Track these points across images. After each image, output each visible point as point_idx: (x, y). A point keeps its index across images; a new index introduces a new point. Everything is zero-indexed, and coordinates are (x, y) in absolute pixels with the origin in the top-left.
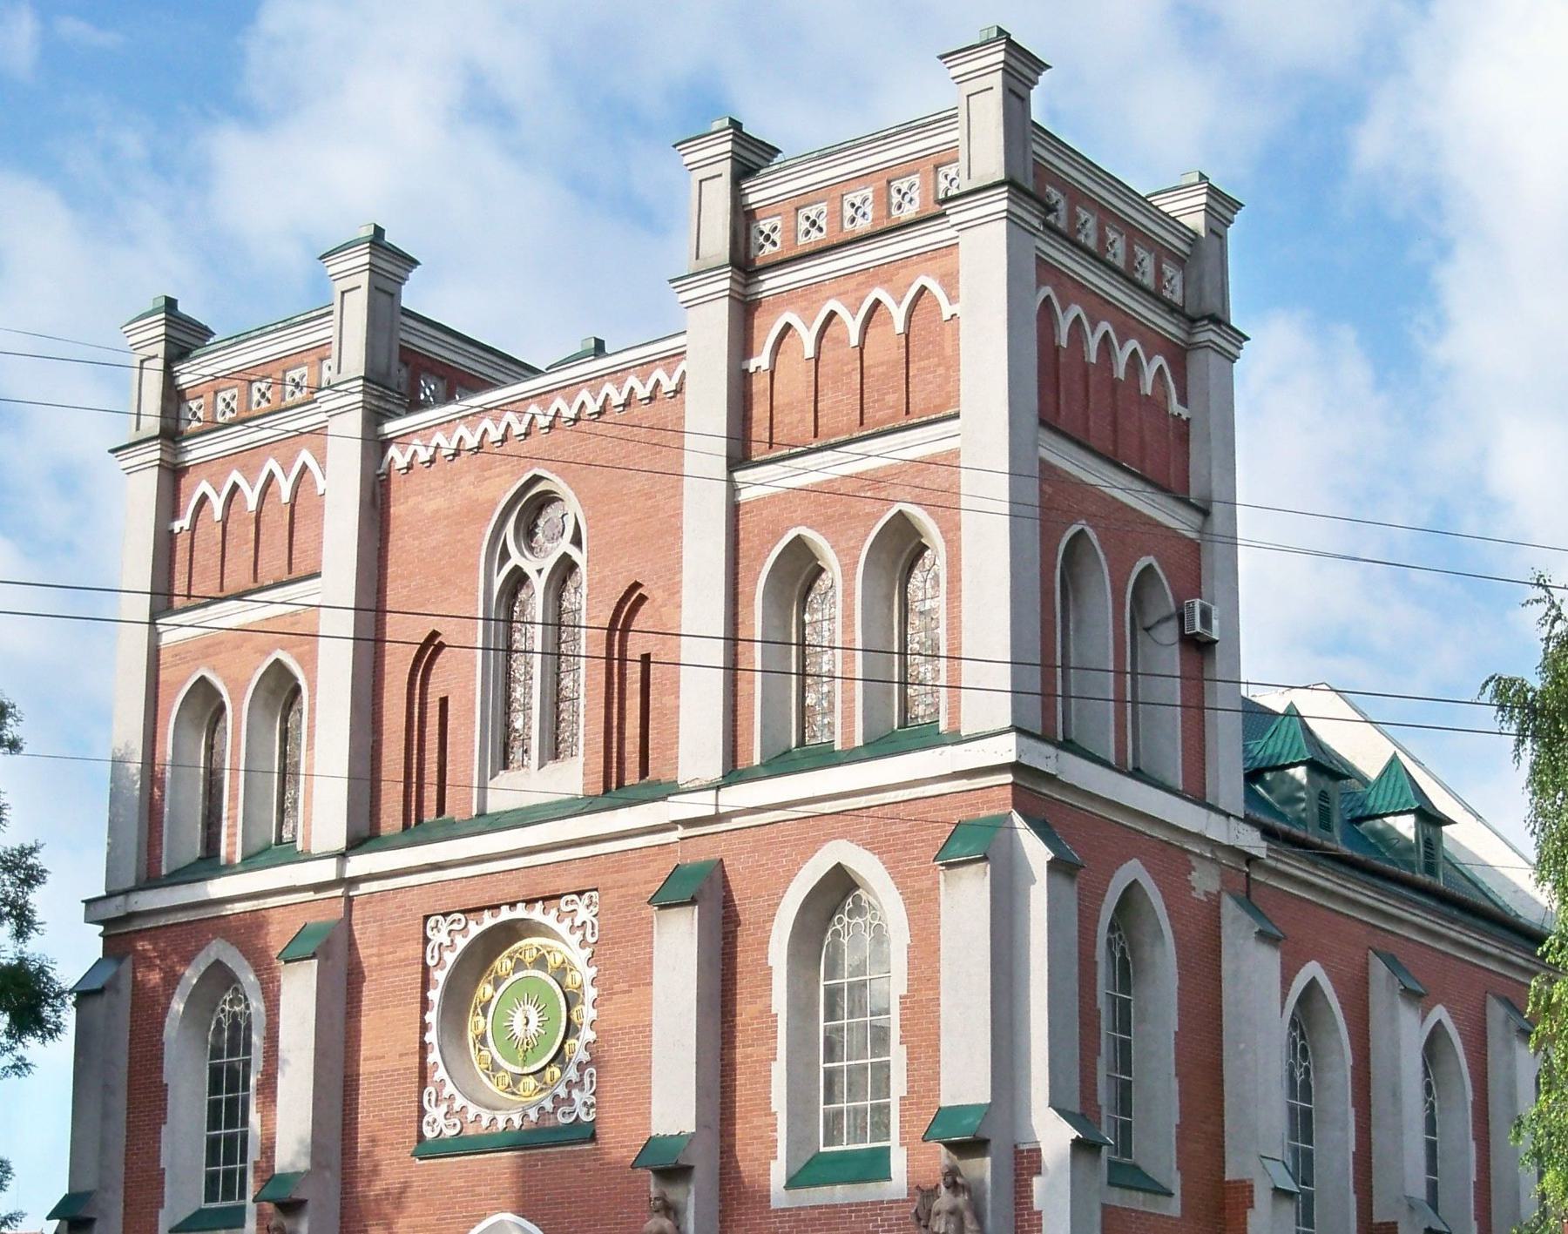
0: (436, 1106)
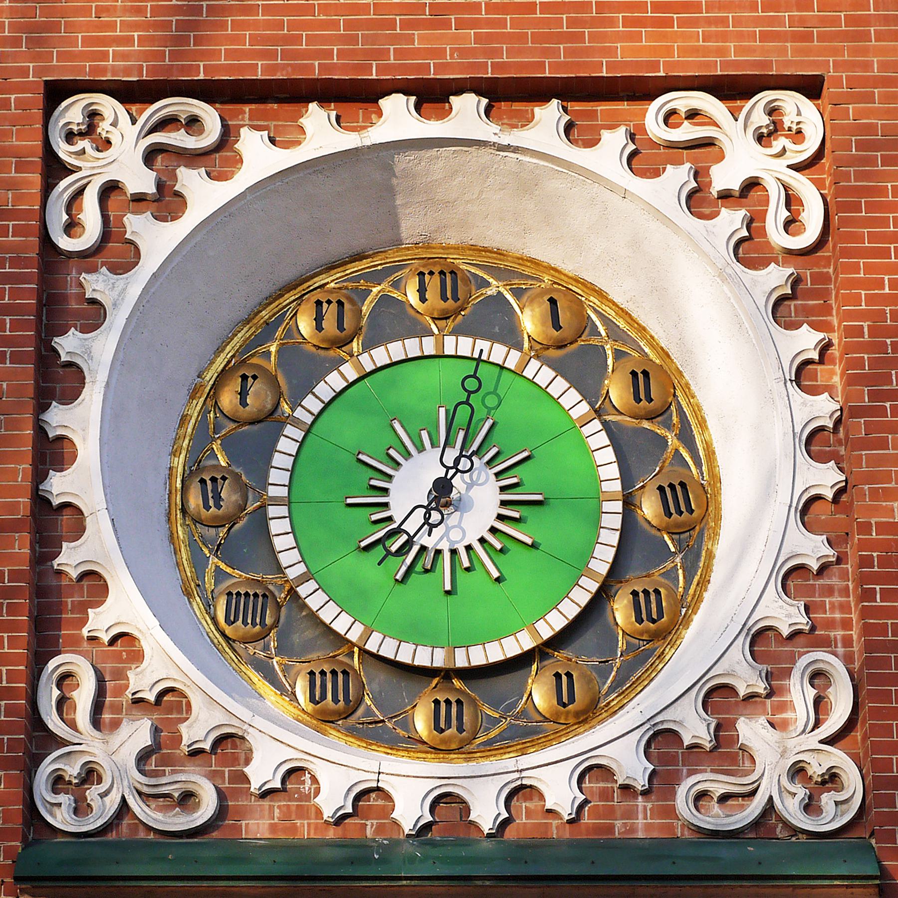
0: (96, 722)
